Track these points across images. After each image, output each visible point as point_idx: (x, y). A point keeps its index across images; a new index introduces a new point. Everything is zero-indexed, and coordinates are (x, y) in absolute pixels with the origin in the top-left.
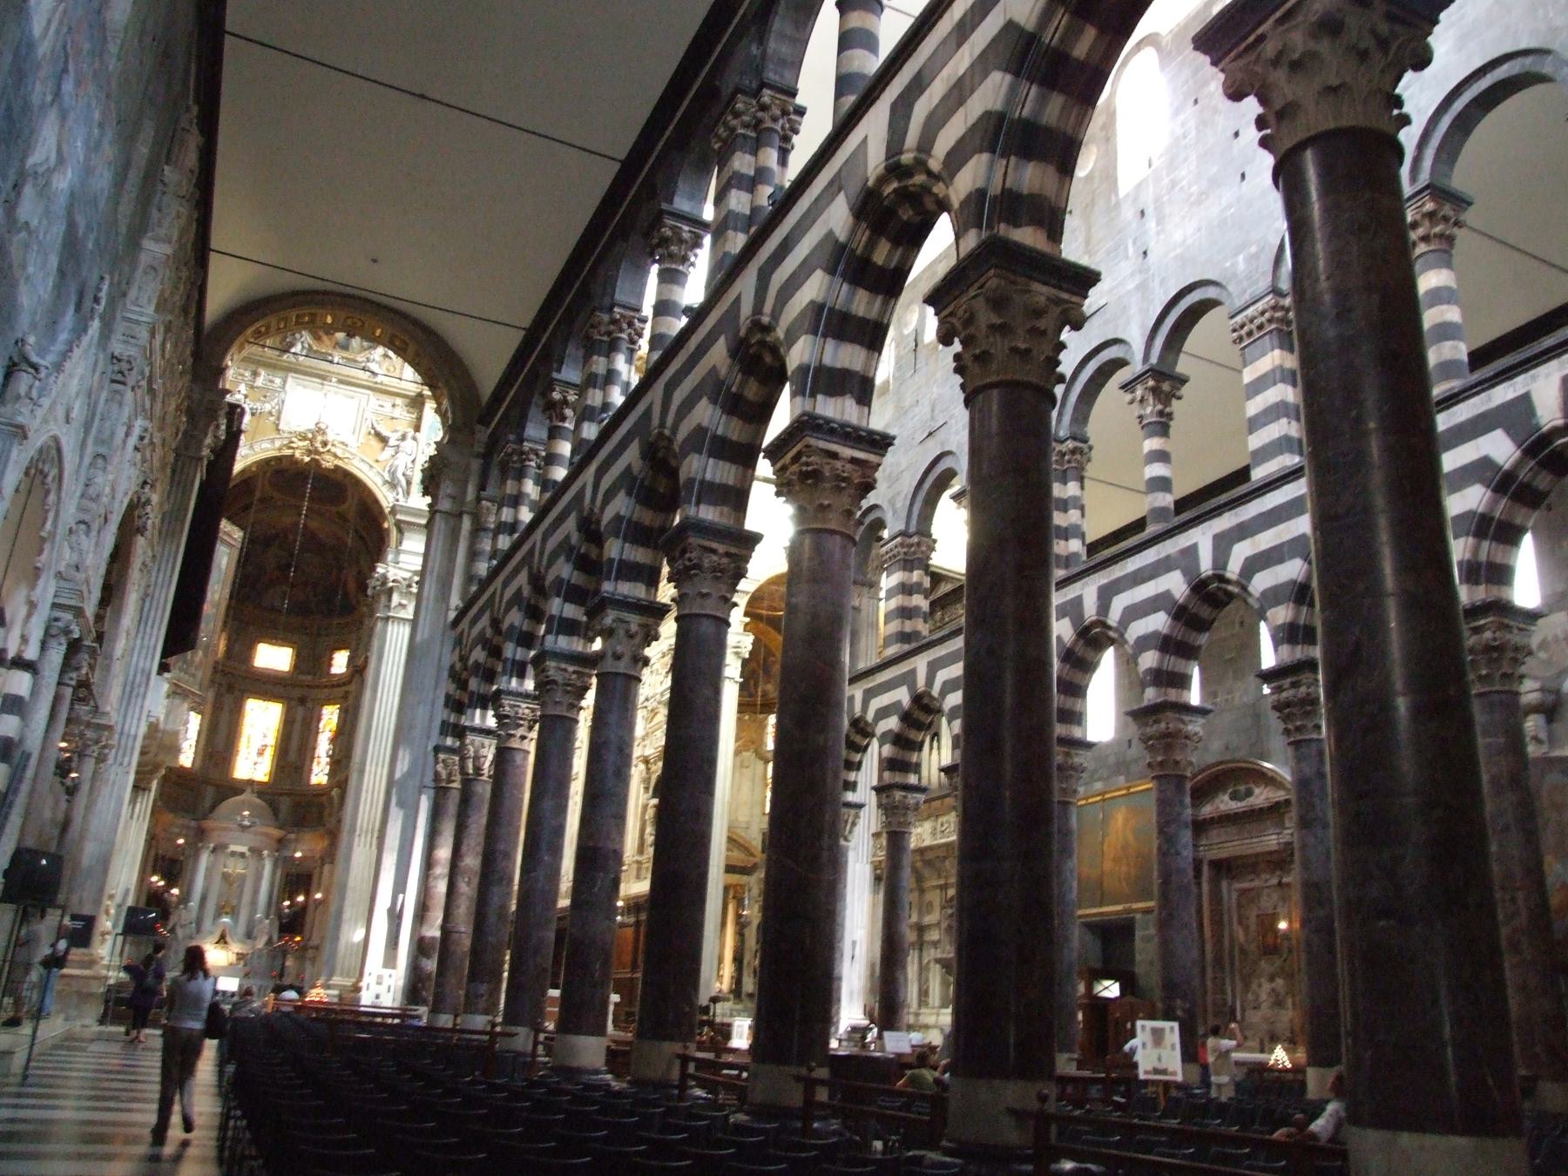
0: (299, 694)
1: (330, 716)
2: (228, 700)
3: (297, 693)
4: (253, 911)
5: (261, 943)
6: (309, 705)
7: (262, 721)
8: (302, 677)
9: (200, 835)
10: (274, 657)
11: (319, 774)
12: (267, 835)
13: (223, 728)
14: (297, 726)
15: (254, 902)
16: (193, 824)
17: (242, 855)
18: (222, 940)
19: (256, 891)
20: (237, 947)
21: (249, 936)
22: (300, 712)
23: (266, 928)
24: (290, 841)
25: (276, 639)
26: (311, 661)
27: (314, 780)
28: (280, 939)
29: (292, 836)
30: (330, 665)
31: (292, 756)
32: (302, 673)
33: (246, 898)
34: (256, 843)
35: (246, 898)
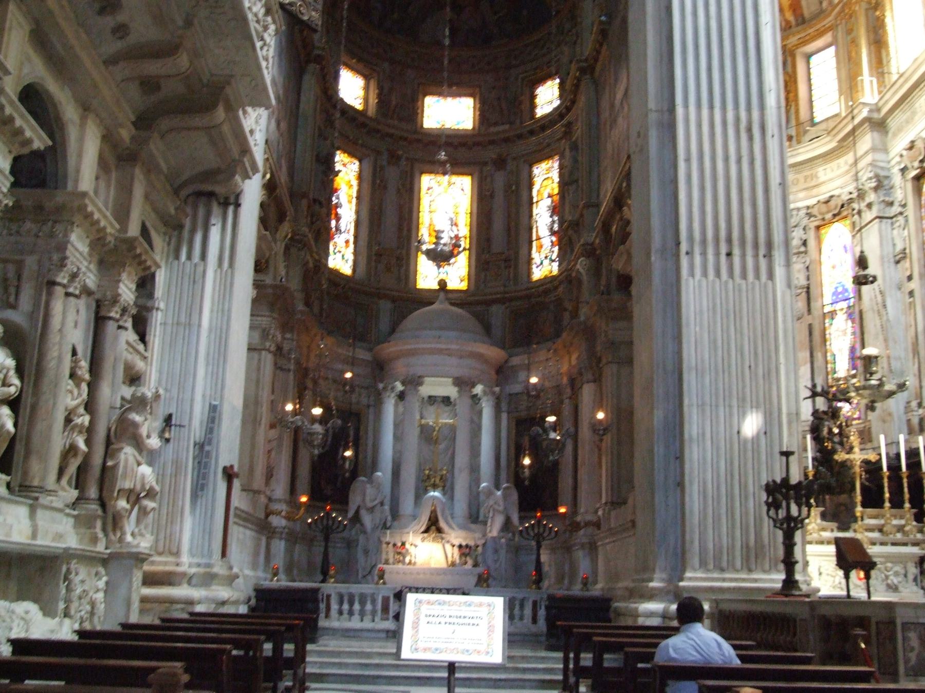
0: (494, 158)
1: (546, 178)
2: (392, 174)
3: (491, 153)
4: (475, 480)
5: (494, 529)
6: (511, 165)
7: (446, 203)
8: (493, 129)
9: (380, 369)
10: (449, 112)
11: (544, 263)
12: (479, 357)
13: (390, 218)
14: (499, 201)
15: (474, 469)
16: (362, 354)
17: (446, 400)
18: (433, 527)
19: (475, 451)
20: (456, 537)
21: (475, 518)
22: (500, 180)
23: (500, 502)
24: (515, 370)
25: (451, 86)
26: (504, 110)
27: (538, 274)
28: (521, 523)
29: (515, 361)
30: (533, 106)
31: (499, 243)
32: (496, 124)
33: (462, 459)
34: (465, 368)
35: (462, 459)
